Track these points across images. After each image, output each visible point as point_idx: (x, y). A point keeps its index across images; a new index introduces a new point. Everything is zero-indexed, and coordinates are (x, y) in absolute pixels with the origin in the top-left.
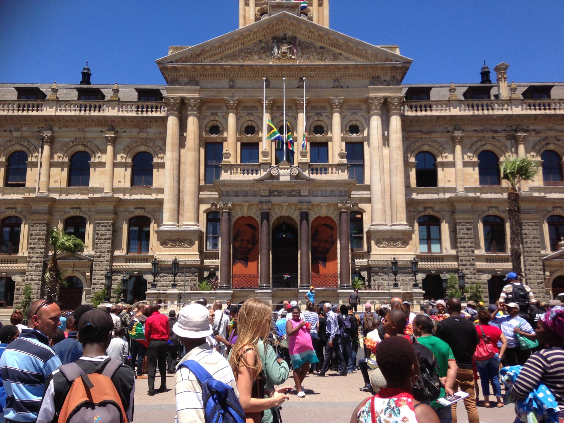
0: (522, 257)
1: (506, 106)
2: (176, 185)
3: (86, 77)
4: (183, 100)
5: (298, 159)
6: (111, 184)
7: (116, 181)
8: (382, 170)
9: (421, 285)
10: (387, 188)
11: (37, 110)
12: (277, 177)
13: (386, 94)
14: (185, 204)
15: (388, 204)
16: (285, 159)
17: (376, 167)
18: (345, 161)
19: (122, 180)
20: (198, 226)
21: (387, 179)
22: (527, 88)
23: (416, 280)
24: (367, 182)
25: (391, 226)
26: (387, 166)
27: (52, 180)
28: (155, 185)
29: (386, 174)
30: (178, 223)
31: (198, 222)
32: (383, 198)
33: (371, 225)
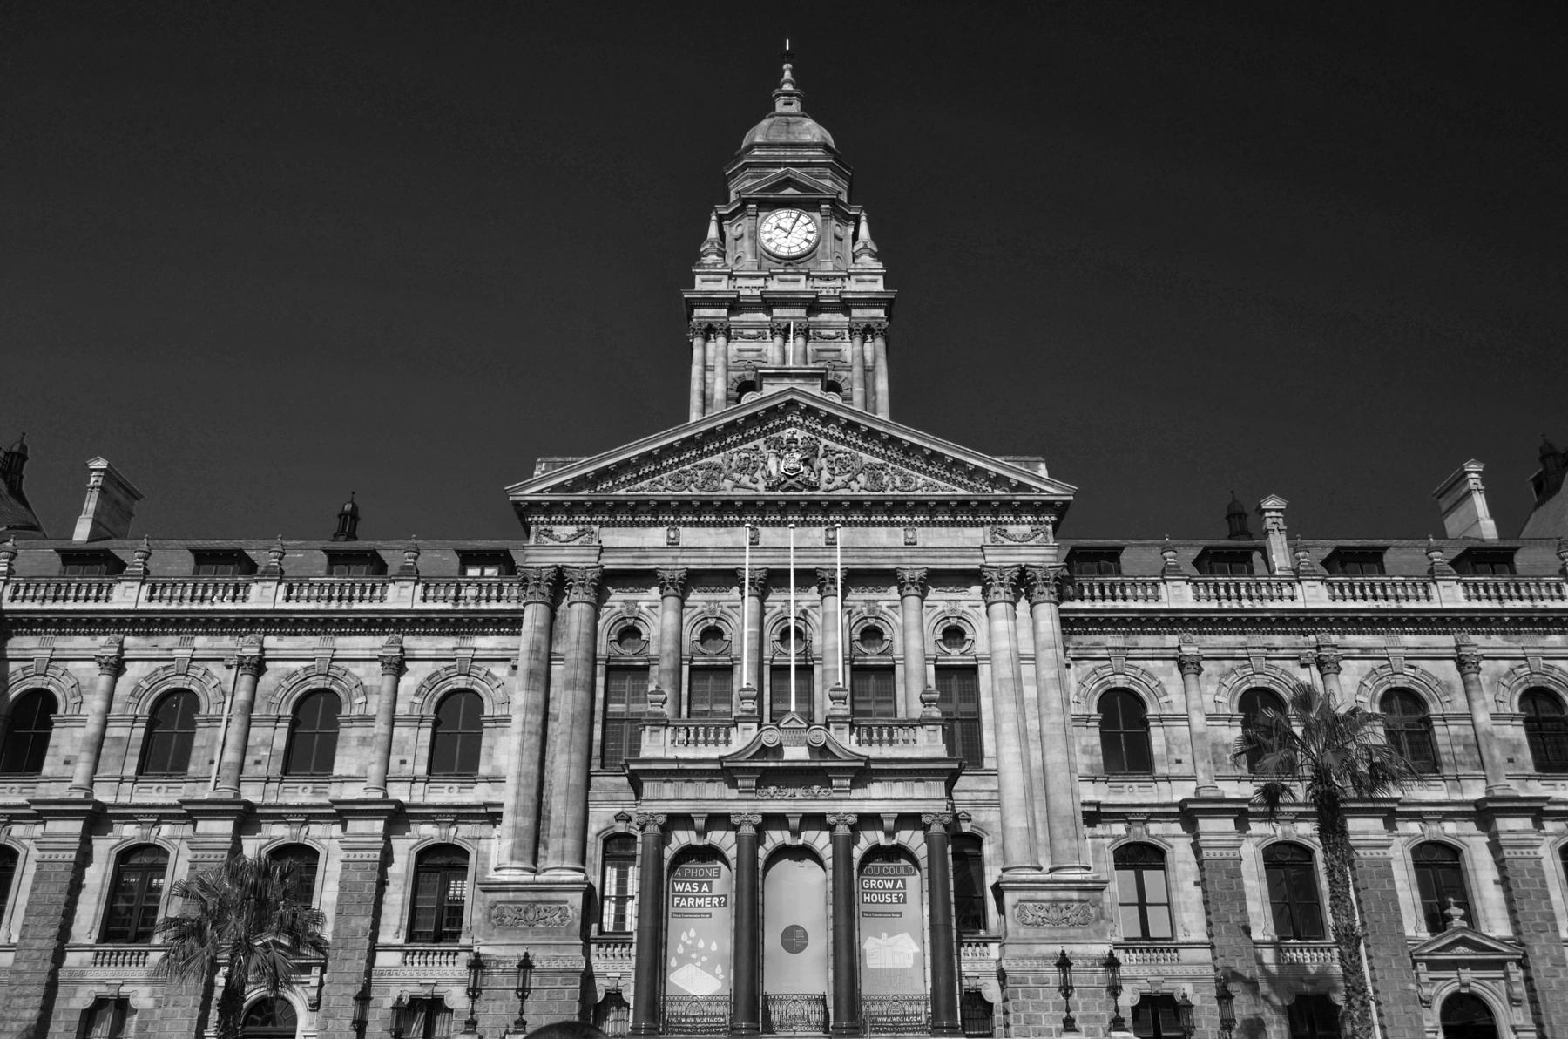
0: (1362, 948)
1: (1286, 591)
2: (534, 768)
3: (349, 523)
4: (560, 571)
5: (824, 705)
6: (383, 768)
7: (394, 760)
8: (1023, 735)
9: (1129, 1023)
10: (1037, 775)
11: (234, 599)
12: (777, 751)
13: (1022, 560)
14: (553, 816)
15: (1040, 815)
16: (793, 708)
17: (1009, 727)
18: (936, 713)
19: (410, 760)
20: (583, 871)
21: (1036, 756)
22: (1329, 551)
23: (1117, 1010)
24: (988, 764)
25: (1051, 871)
26: (1033, 724)
27: (249, 760)
28: (484, 769)
29: (1032, 746)
30: (535, 862)
31: (583, 862)
32: (1030, 798)
33: (1004, 870)
